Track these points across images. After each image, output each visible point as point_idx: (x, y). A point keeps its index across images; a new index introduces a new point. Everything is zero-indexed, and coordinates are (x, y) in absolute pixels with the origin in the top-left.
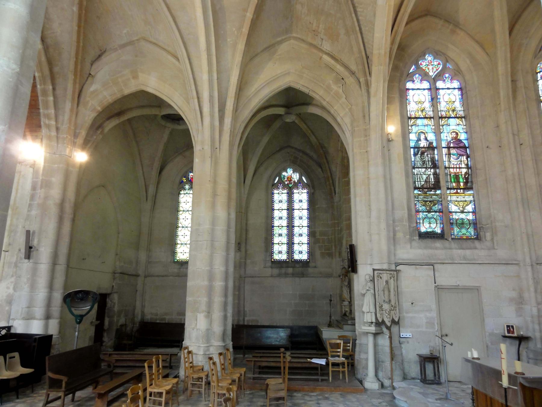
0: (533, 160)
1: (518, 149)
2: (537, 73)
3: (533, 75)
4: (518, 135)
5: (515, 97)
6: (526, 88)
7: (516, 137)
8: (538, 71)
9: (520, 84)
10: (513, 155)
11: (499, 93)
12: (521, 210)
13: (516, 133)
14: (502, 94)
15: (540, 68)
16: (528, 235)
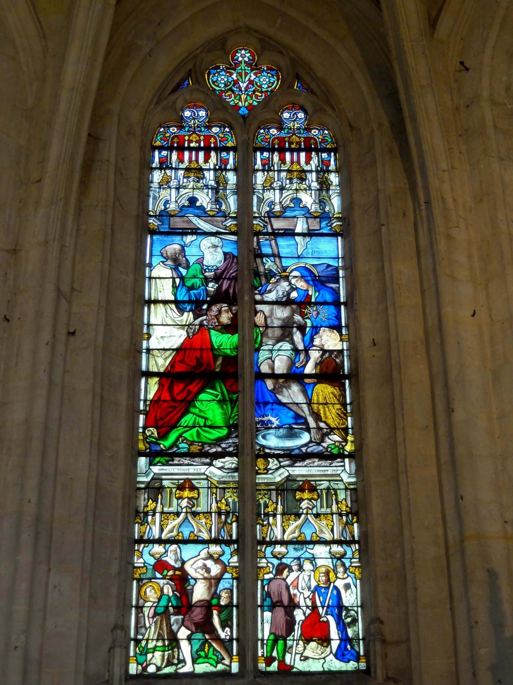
0: (94, 394)
1: (60, 347)
2: (154, 148)
3: (142, 148)
4: (69, 302)
5: (84, 184)
6: (118, 171)
7: (64, 305)
8: (158, 143)
9: (108, 151)
10: (44, 353)
11: (45, 147)
12: (25, 557)
13: (65, 288)
14: (54, 151)
15: (165, 139)
16: (26, 659)
